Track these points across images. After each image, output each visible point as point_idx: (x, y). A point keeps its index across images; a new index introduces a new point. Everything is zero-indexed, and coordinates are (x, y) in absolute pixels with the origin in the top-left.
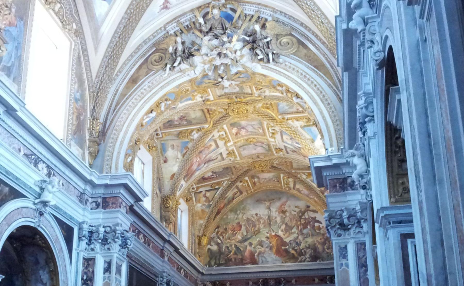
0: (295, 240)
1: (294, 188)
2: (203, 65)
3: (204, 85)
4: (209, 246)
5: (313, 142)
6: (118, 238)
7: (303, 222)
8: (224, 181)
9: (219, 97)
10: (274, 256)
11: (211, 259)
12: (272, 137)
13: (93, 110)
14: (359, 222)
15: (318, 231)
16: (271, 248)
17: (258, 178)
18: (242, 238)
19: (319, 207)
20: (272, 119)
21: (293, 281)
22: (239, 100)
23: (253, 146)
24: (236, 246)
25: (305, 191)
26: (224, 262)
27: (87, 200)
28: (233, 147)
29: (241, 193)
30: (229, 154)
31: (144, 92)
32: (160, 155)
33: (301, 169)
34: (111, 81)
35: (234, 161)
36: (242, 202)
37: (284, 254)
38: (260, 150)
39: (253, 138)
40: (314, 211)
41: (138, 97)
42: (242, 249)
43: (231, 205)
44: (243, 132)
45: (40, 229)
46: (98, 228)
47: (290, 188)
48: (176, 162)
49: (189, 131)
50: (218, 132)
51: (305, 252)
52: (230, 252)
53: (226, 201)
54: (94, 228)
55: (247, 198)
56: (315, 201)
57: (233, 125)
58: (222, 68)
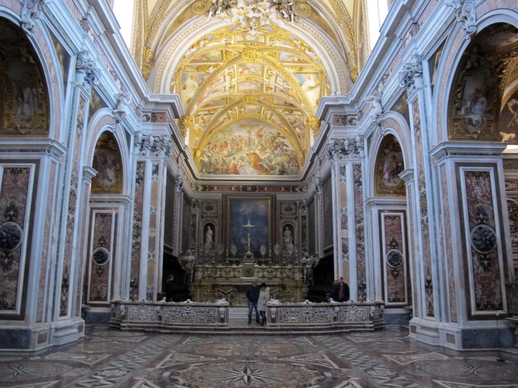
0: (268, 158)
1: (270, 119)
2: (238, 16)
3: (235, 31)
4: (202, 158)
5: (301, 86)
7: (275, 145)
8: (219, 108)
10: (252, 169)
11: (203, 167)
12: (268, 78)
13: (147, 41)
14: (356, 149)
16: (250, 163)
17: (245, 108)
19: (287, 134)
20: (274, 65)
21: (266, 189)
22: (253, 47)
23: (249, 83)
24: (223, 159)
25: (279, 122)
26: (213, 171)
28: (236, 83)
29: (229, 118)
30: (230, 88)
31: (190, 31)
32: (181, 83)
34: (162, 18)
36: (229, 125)
38: (253, 87)
40: (283, 138)
41: (184, 35)
42: (227, 161)
43: (221, 127)
44: (246, 72)
45: (115, 135)
46: (149, 137)
47: (266, 118)
48: (193, 89)
50: (229, 69)
52: (218, 164)
53: (217, 124)
54: (146, 137)
55: (233, 122)
56: (285, 130)
57: (241, 65)
58: (254, 20)
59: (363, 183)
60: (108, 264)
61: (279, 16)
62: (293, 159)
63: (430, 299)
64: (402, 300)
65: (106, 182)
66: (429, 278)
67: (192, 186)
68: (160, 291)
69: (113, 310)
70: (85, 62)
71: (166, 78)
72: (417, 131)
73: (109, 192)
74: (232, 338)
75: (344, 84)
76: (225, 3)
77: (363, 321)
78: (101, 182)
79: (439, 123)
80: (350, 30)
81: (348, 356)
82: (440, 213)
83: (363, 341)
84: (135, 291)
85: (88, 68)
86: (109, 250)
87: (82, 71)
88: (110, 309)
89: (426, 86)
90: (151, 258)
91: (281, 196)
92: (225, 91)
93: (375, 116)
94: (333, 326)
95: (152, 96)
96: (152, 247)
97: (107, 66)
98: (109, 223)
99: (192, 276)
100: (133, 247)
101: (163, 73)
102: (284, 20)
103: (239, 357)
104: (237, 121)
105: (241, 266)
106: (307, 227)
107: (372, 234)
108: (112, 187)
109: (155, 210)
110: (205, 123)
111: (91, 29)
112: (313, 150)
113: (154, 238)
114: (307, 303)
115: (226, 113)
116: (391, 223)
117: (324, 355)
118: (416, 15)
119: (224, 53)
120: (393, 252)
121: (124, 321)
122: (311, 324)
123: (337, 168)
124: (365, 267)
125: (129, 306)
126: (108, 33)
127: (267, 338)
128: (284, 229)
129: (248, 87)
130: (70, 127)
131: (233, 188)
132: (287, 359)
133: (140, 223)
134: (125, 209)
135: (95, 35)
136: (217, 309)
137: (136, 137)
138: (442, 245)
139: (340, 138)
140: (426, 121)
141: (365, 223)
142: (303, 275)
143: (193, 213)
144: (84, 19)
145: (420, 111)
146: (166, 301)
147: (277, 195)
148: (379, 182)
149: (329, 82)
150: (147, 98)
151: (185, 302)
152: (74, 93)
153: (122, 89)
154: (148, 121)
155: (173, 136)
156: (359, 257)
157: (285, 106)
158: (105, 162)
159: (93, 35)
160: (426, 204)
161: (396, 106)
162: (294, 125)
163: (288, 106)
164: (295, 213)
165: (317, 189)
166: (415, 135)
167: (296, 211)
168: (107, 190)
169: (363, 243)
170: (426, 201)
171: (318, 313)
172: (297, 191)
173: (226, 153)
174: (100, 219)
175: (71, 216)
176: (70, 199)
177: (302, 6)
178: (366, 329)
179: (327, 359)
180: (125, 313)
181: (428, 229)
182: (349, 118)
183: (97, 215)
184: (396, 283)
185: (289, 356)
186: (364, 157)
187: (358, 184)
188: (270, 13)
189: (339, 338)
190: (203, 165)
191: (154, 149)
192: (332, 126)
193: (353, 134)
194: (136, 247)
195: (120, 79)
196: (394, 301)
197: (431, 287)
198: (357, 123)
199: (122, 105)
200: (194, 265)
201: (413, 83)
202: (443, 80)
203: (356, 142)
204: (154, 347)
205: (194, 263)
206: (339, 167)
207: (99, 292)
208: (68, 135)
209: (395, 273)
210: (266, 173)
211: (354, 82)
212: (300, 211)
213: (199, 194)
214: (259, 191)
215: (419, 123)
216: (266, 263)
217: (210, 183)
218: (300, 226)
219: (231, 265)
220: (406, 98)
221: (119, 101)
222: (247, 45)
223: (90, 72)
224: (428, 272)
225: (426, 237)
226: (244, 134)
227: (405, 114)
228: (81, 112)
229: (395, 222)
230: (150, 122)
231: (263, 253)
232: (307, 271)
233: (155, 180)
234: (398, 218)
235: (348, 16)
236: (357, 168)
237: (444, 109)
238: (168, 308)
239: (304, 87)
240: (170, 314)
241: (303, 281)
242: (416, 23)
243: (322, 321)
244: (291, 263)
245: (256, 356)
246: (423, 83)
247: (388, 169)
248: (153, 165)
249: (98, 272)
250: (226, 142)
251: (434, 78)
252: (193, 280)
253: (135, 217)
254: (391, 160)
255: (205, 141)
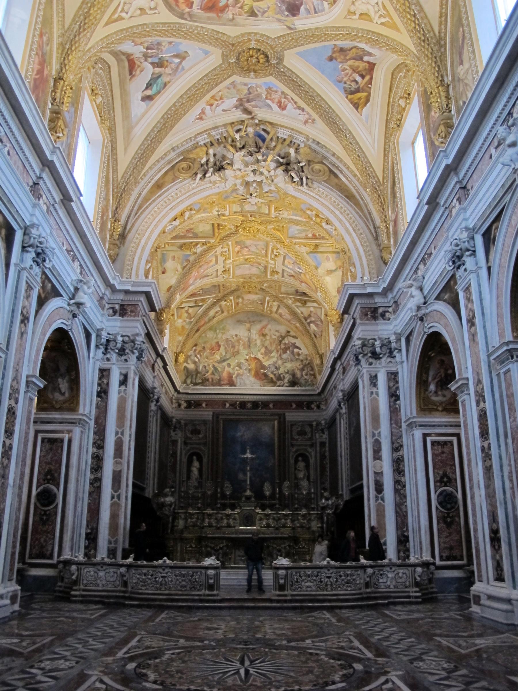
0: (274, 364)
1: (276, 312)
2: (234, 179)
3: (230, 199)
4: (185, 364)
6: (136, 349)
7: (283, 347)
8: (209, 299)
9: (235, 213)
10: (252, 379)
11: (187, 377)
12: (272, 259)
13: (116, 211)
15: (297, 357)
16: (250, 370)
17: (243, 298)
18: (221, 358)
19: (299, 333)
20: (281, 242)
21: (271, 406)
22: (253, 219)
23: (249, 266)
24: (214, 366)
25: (288, 316)
26: (200, 381)
27: (105, 306)
28: (231, 266)
29: (223, 312)
31: (171, 198)
32: (159, 265)
33: (288, 294)
34: (136, 183)
35: (227, 279)
36: (222, 320)
37: (263, 378)
38: (254, 271)
39: (253, 258)
41: (164, 204)
42: (220, 370)
43: (211, 323)
44: (245, 251)
45: (70, 333)
46: (116, 337)
47: (271, 312)
49: (194, 244)
50: (222, 248)
51: (284, 377)
52: (208, 372)
53: (207, 319)
54: (111, 337)
55: (227, 317)
56: (296, 327)
57: (237, 243)
58: (255, 185)
59: (402, 397)
60: (56, 507)
61: (287, 180)
62: (308, 365)
63: (498, 557)
64: (459, 557)
65: (57, 396)
66: (495, 526)
67: (172, 402)
68: (127, 545)
69: (61, 572)
70: (34, 238)
71: (140, 259)
72: (471, 327)
73: (60, 409)
74: (224, 612)
75: (374, 266)
76: (218, 163)
77: (406, 587)
78: (51, 396)
79: (499, 316)
80: (379, 196)
81: (386, 639)
82: (506, 436)
83: (406, 617)
84: (92, 545)
85: (37, 247)
86: (58, 489)
87: (29, 249)
88: (57, 570)
89: (481, 268)
90: (116, 499)
91: (292, 416)
92: (217, 276)
93: (415, 308)
94: (365, 596)
95: (121, 283)
96: (116, 485)
97: (63, 244)
98: (59, 451)
99: (170, 525)
100: (91, 484)
101: (135, 252)
102: (294, 184)
103: (233, 640)
104: (232, 316)
105: (237, 511)
106: (328, 457)
107: (415, 466)
108: (64, 402)
109: (122, 434)
110: (191, 318)
111: (44, 196)
112: (334, 354)
113: (120, 471)
114: (328, 563)
115: (218, 306)
116: (440, 451)
117: (352, 638)
118: (464, 176)
119: (216, 227)
120: (444, 491)
121: (75, 588)
122: (334, 592)
123: (366, 378)
124: (406, 512)
125: (83, 567)
126: (65, 202)
127: (272, 612)
128: (296, 461)
129: (247, 270)
130: (12, 322)
131: (228, 405)
132: (300, 644)
133: (101, 451)
134: (82, 432)
135: (48, 203)
136: (203, 571)
137: (98, 336)
138: (511, 481)
139: (369, 338)
140: (483, 313)
141: (405, 452)
142: (322, 523)
143: (173, 438)
144: (35, 184)
145: (474, 300)
146: (134, 559)
147: (287, 414)
148: (422, 395)
149: (354, 264)
150: (114, 285)
151: (160, 562)
152: (19, 278)
153: (81, 273)
154: (114, 315)
155: (148, 335)
156: (398, 499)
157: (296, 295)
158: (57, 369)
159: (45, 203)
160: (487, 425)
161: (442, 295)
162: (309, 321)
163: (300, 295)
164: (311, 439)
165: (340, 405)
166: (469, 332)
167: (312, 435)
168: (57, 406)
169: (403, 479)
170: (487, 420)
171: (343, 578)
172: (313, 409)
173: (218, 358)
174: (48, 446)
175: (8, 442)
176: (7, 418)
177: (317, 167)
178: (411, 600)
179: (357, 643)
180: (77, 577)
181: (490, 459)
182: (381, 310)
183: (43, 440)
184: (450, 534)
185: (303, 640)
186: (402, 362)
187: (394, 398)
188: (276, 176)
189: (374, 612)
190: (188, 373)
191: (122, 352)
192: (358, 321)
193: (386, 332)
194: (95, 485)
195: (79, 261)
196: (448, 559)
197: (499, 540)
198: (392, 317)
199: (80, 294)
200: (174, 509)
201: (464, 264)
202: (503, 260)
203: (390, 342)
204: (116, 625)
205: (173, 506)
206: (369, 376)
207: (42, 547)
208: (8, 333)
209: (449, 520)
210: (272, 384)
211: (385, 263)
212: (317, 435)
213: (182, 413)
214: (262, 408)
215: (474, 316)
216: (272, 507)
217: (196, 397)
218: (318, 455)
219: (224, 510)
220: (456, 283)
221: (77, 289)
222: (246, 217)
223: (40, 250)
224: (493, 517)
225: (488, 470)
226: (242, 332)
227: (455, 304)
228: (27, 303)
229: (446, 450)
230: (117, 317)
231: (268, 493)
232: (327, 518)
233: (122, 394)
234: (449, 444)
235: (376, 179)
236: (393, 377)
237: (506, 298)
238: (137, 570)
239: (321, 271)
240: (138, 579)
241: (323, 531)
242: (464, 188)
243: (349, 589)
244: (306, 507)
245: (258, 639)
246: (477, 264)
247: (434, 379)
248: (121, 374)
249: (41, 519)
250: (218, 343)
251: (491, 257)
252: (172, 530)
253: (94, 443)
254: (438, 365)
255: (191, 342)
